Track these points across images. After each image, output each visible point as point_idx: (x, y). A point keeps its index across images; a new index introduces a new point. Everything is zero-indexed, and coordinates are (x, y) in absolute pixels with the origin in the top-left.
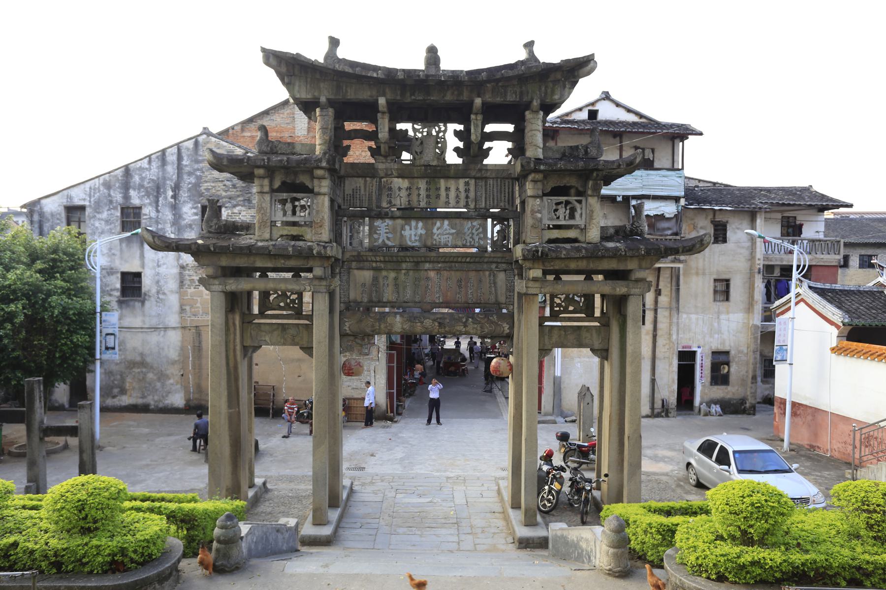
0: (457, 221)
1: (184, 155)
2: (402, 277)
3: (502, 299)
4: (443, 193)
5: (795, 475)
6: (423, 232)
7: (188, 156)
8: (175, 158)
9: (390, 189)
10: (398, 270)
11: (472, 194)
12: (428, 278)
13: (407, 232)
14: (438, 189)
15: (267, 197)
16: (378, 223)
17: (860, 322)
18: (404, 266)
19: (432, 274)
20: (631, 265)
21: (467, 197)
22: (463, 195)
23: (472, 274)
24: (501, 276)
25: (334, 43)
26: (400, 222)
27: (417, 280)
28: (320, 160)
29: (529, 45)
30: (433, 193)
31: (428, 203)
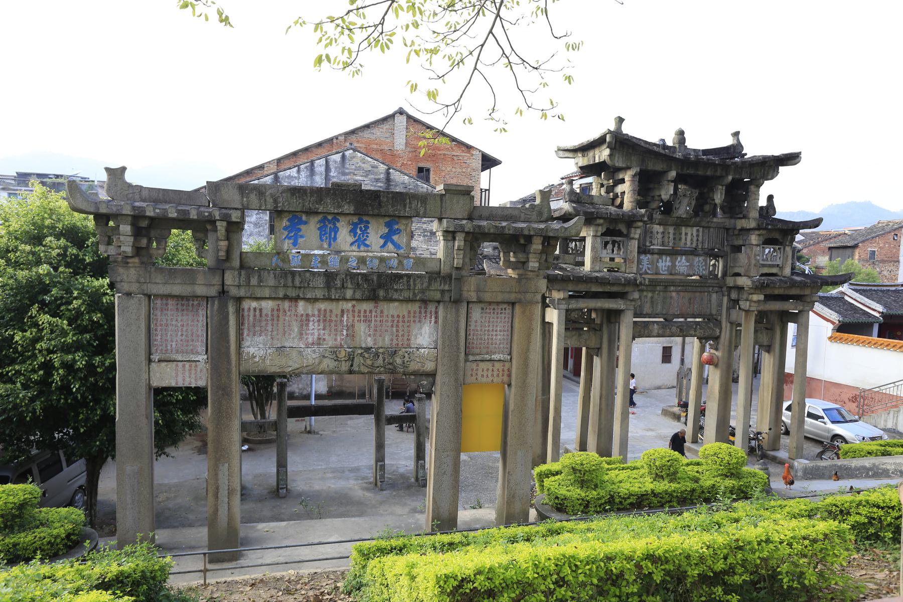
0: (691, 257)
1: (331, 167)
2: (656, 296)
3: (714, 312)
4: (683, 236)
5: (860, 422)
6: (670, 264)
7: (336, 168)
8: (323, 169)
9: (652, 232)
10: (653, 291)
11: (700, 239)
12: (671, 297)
13: (660, 264)
14: (681, 234)
15: (599, 239)
16: (642, 257)
17: (847, 320)
18: (658, 288)
19: (674, 294)
20: (807, 292)
21: (697, 240)
22: (695, 239)
23: (698, 294)
24: (714, 296)
25: (620, 120)
26: (656, 256)
27: (665, 298)
28: (643, 216)
29: (736, 134)
30: (677, 237)
31: (674, 243)
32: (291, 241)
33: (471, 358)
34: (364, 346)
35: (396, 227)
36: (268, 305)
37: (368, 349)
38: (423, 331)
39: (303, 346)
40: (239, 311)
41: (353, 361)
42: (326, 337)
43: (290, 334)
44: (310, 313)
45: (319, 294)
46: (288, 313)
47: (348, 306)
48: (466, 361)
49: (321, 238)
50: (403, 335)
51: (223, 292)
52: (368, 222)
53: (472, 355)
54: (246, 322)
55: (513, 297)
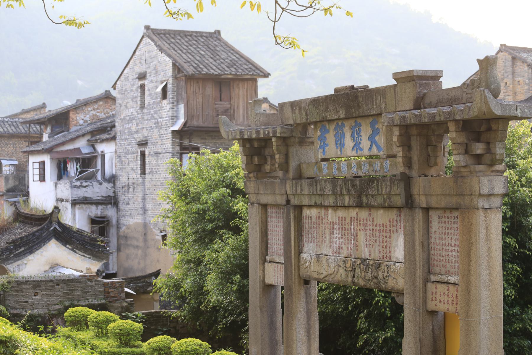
32: (322, 150)
33: (433, 278)
34: (363, 257)
35: (377, 127)
36: (314, 212)
37: (364, 260)
38: (399, 243)
39: (331, 255)
40: (299, 219)
41: (355, 271)
42: (343, 246)
43: (325, 242)
44: (334, 221)
45: (330, 201)
46: (324, 221)
47: (353, 213)
48: (426, 281)
49: (336, 145)
50: (386, 247)
51: (288, 202)
52: (361, 126)
53: (435, 274)
54: (305, 229)
55: (454, 201)
